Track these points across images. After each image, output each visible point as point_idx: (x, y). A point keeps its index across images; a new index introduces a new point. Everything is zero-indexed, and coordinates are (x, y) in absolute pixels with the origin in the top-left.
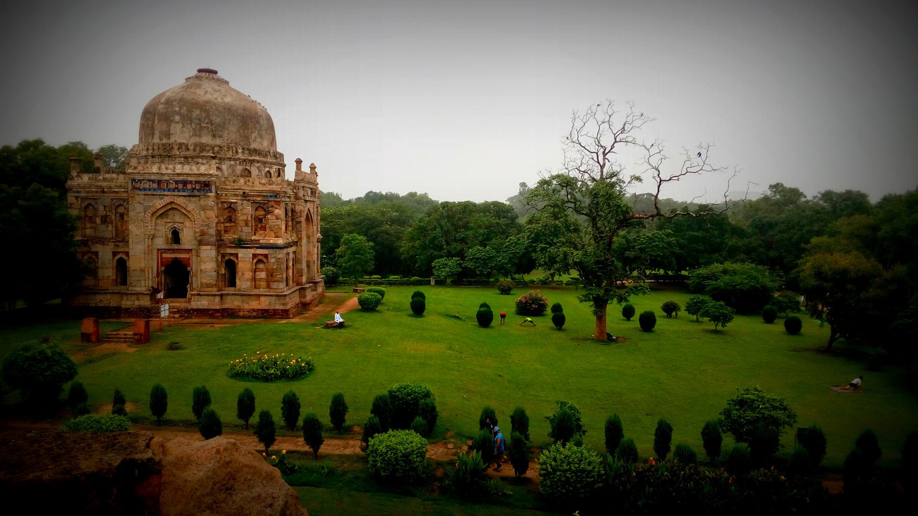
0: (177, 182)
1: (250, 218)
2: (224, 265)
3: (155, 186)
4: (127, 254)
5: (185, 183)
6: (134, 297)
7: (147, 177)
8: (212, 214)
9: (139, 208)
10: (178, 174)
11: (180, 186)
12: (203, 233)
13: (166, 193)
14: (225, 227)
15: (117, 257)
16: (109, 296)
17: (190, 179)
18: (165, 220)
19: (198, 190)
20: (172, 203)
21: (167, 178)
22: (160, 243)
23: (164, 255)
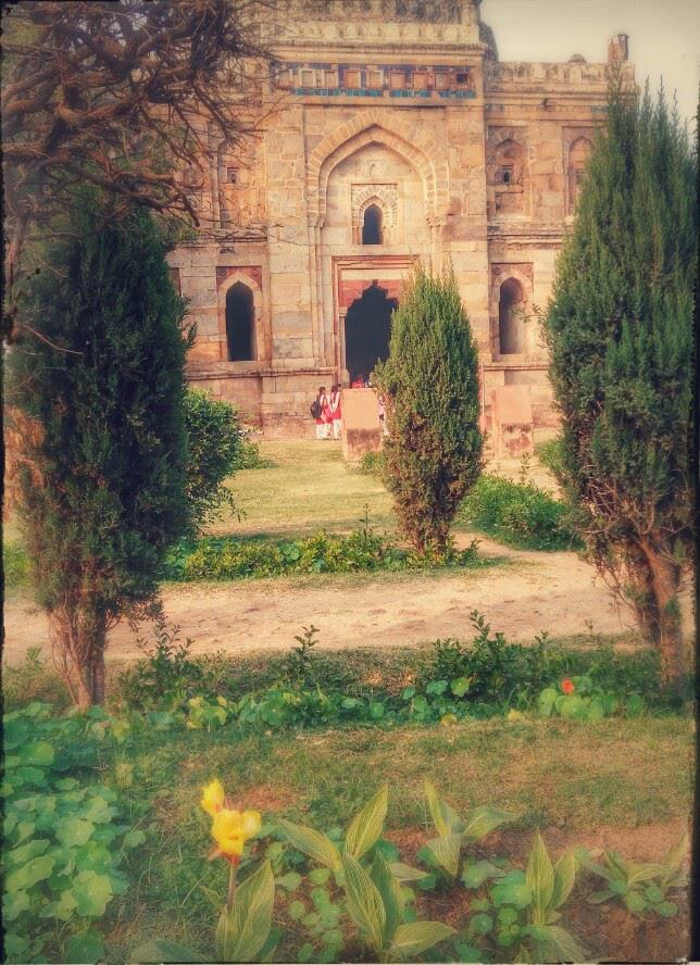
0: (388, 69)
1: (559, 170)
2: (497, 291)
3: (334, 80)
4: (255, 272)
5: (407, 71)
6: (292, 382)
7: (309, 55)
8: (476, 154)
9: (294, 145)
10: (393, 47)
11: (397, 81)
12: (454, 211)
13: (362, 100)
14: (498, 195)
15: (229, 283)
16: (216, 385)
17: (420, 59)
18: (350, 178)
19: (445, 92)
20: (375, 127)
21: (360, 57)
22: (342, 240)
23: (348, 276)
